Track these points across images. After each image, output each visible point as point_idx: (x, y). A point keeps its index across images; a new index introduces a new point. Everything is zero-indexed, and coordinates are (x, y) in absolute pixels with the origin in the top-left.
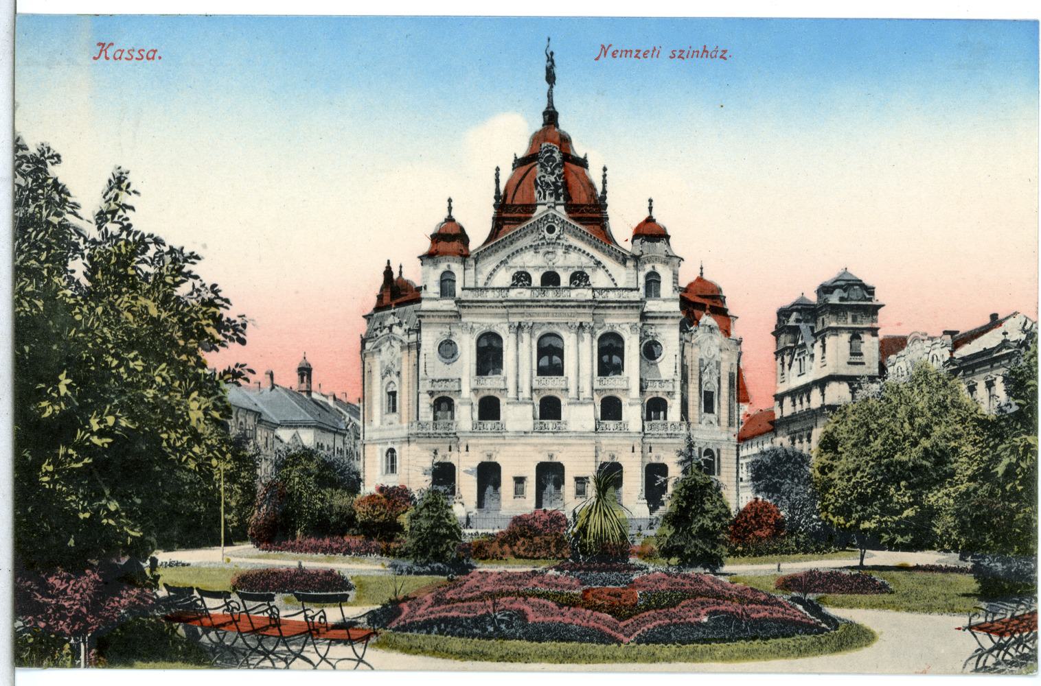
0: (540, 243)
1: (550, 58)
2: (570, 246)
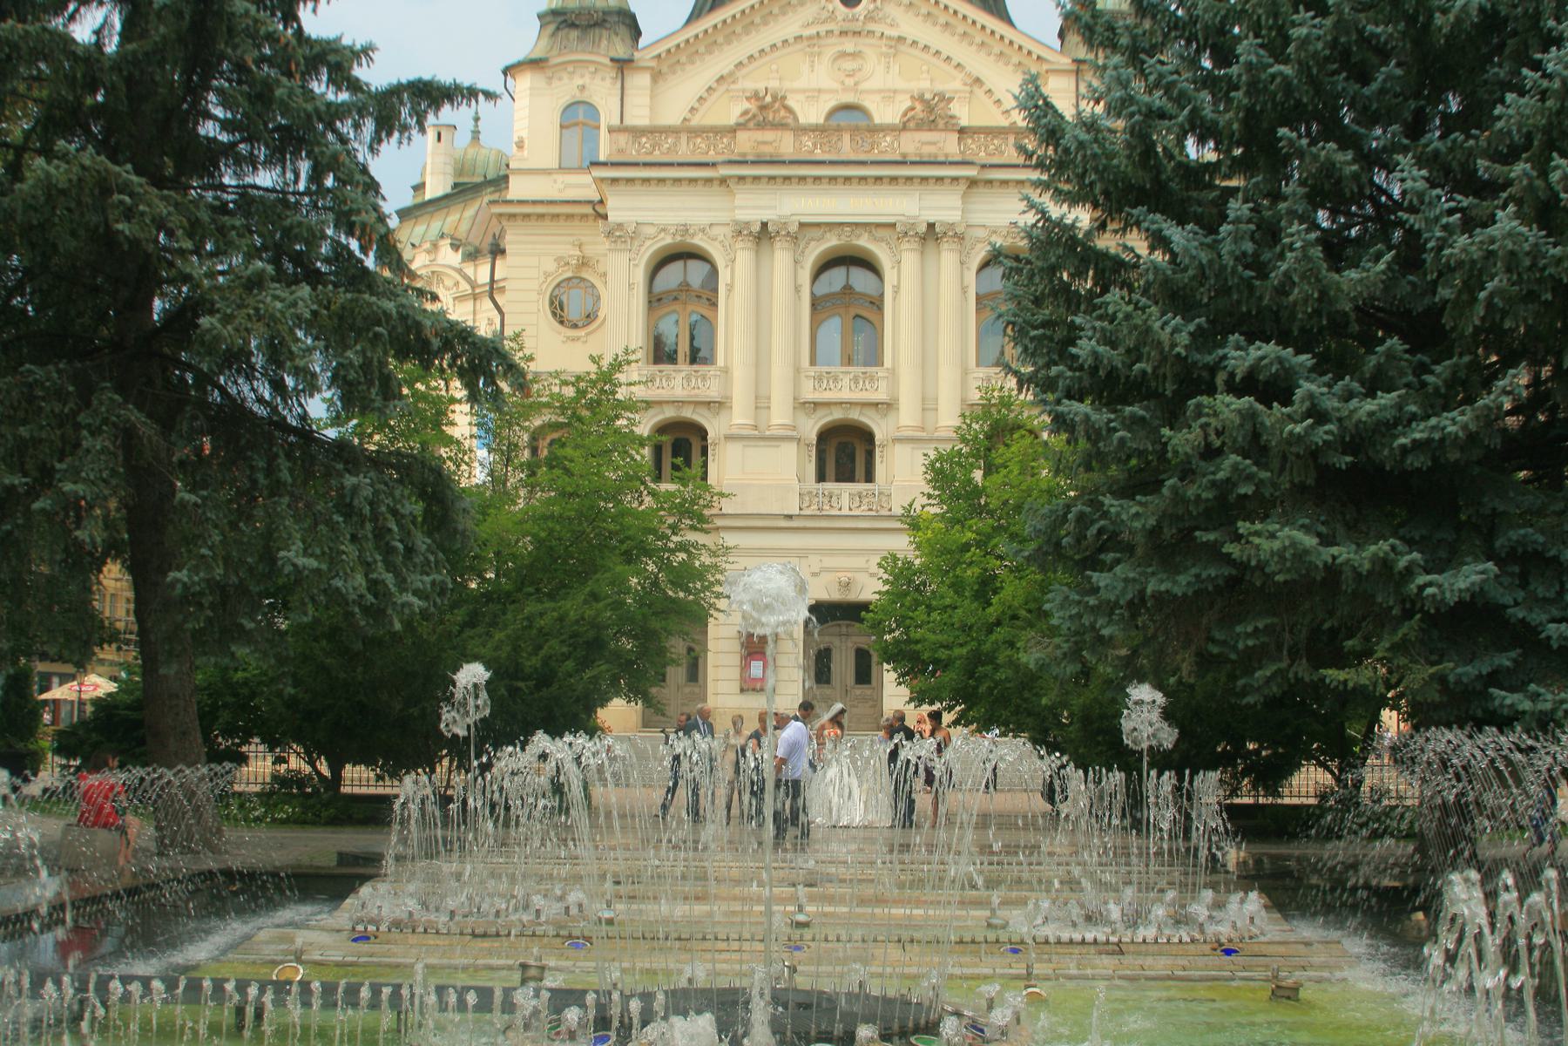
0: (822, 29)
2: (901, 39)
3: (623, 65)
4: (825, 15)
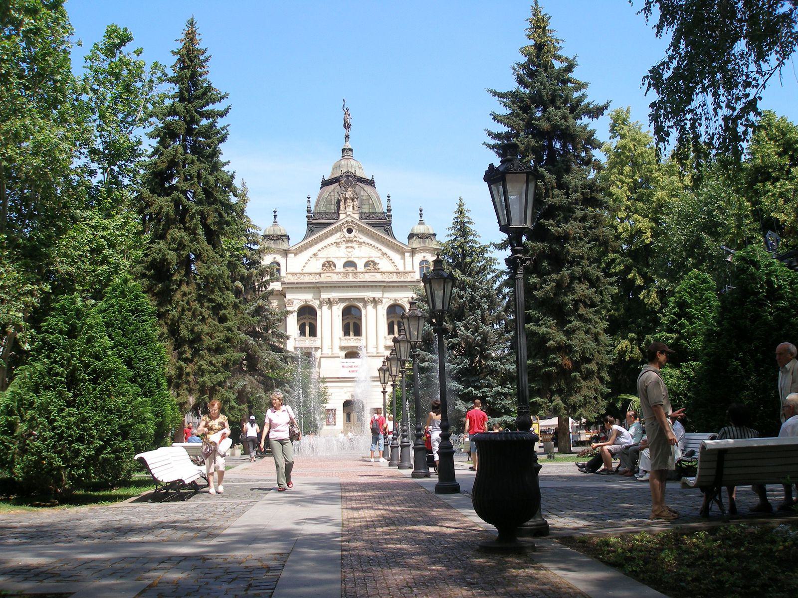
1: (347, 112)
2: (364, 242)
3: (286, 253)
4: (342, 236)
